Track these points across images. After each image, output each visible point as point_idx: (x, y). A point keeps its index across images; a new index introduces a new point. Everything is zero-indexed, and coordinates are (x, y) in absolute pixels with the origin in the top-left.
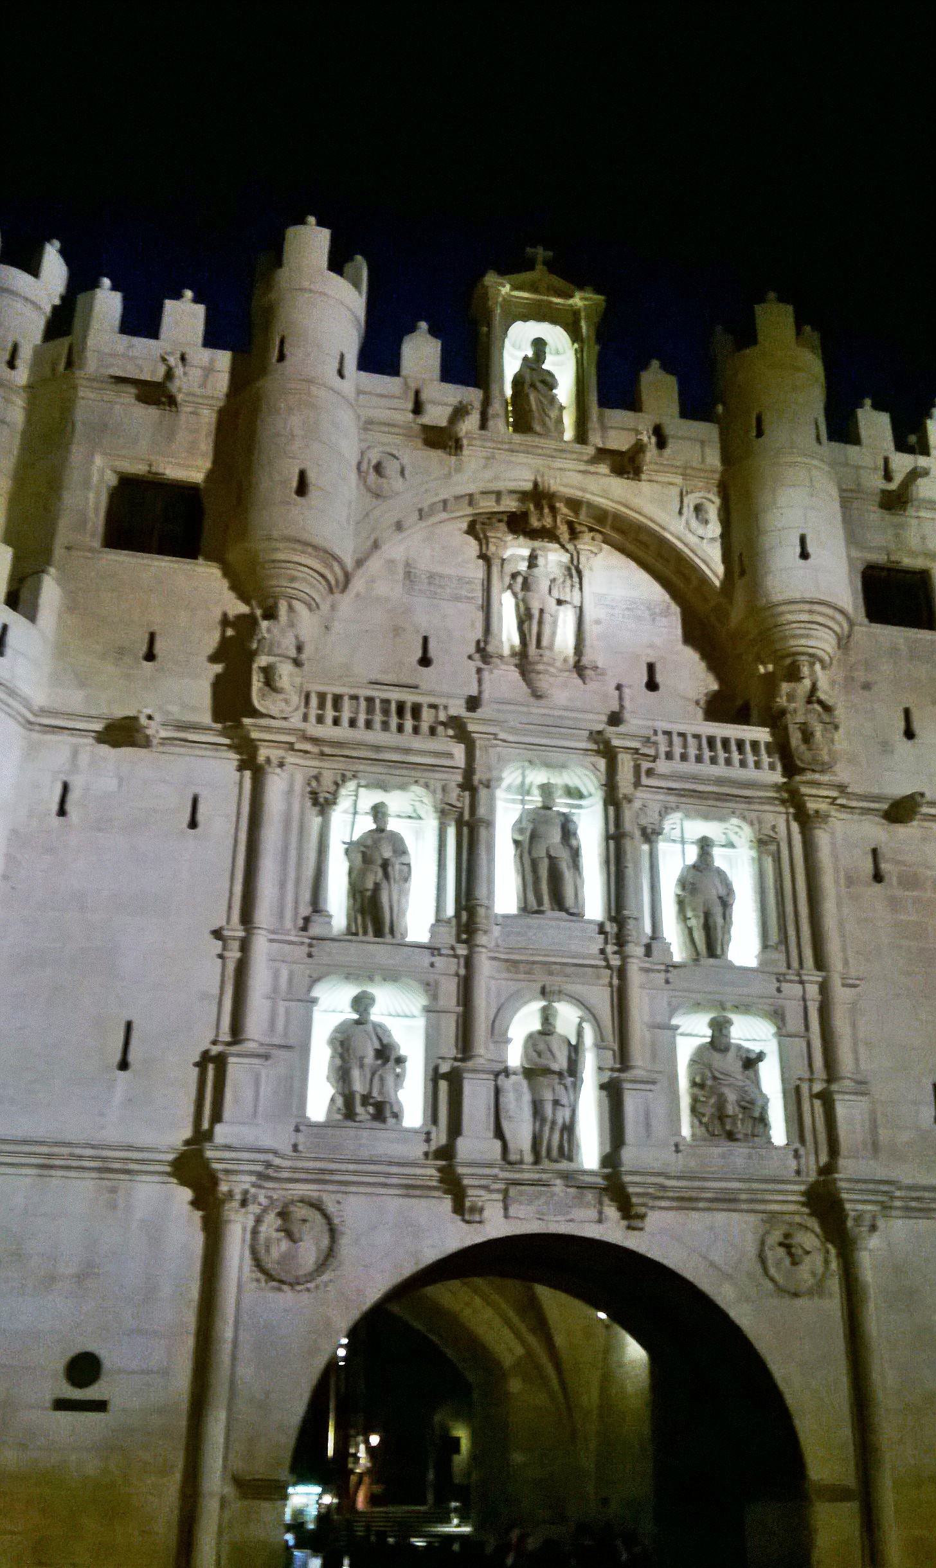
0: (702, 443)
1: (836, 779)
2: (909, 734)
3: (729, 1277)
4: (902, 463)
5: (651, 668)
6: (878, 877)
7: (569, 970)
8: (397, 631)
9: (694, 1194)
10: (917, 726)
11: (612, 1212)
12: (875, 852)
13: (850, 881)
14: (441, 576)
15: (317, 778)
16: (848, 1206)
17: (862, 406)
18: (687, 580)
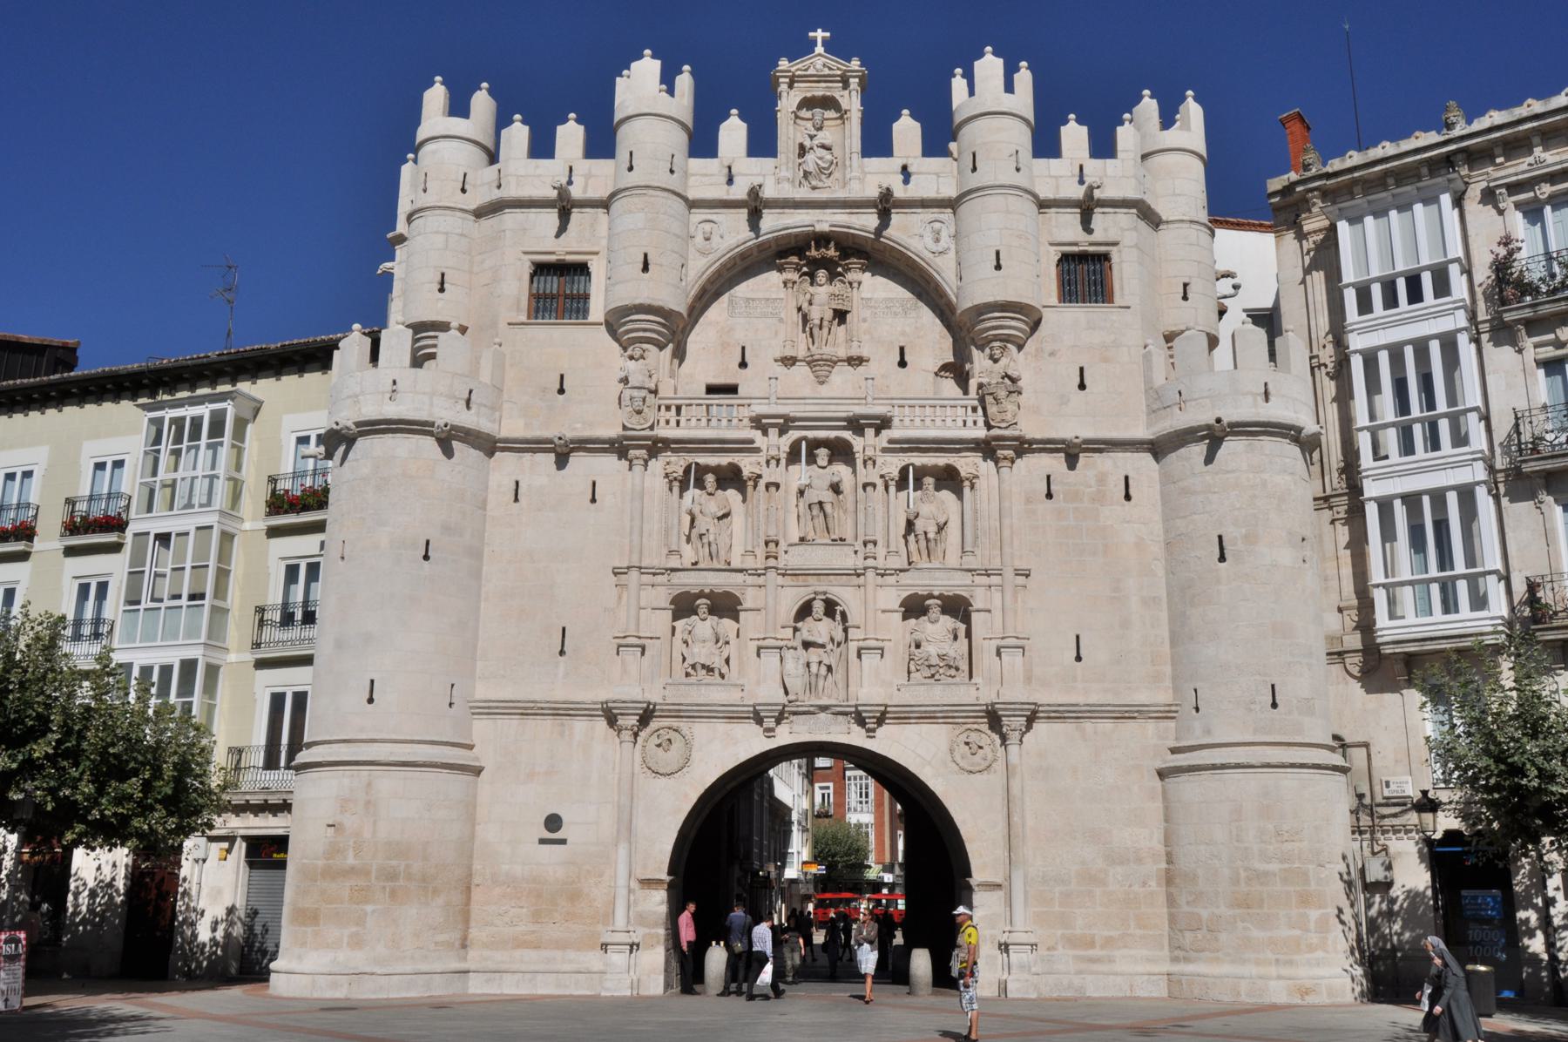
0: (938, 175)
1: (1016, 433)
2: (1082, 386)
3: (929, 763)
4: (1095, 168)
5: (902, 350)
6: (1049, 496)
7: (832, 577)
8: (725, 346)
9: (906, 715)
10: (1087, 382)
11: (856, 728)
12: (1048, 477)
13: (1028, 501)
14: (753, 300)
15: (668, 463)
16: (1003, 719)
17: (1066, 122)
18: (929, 283)
